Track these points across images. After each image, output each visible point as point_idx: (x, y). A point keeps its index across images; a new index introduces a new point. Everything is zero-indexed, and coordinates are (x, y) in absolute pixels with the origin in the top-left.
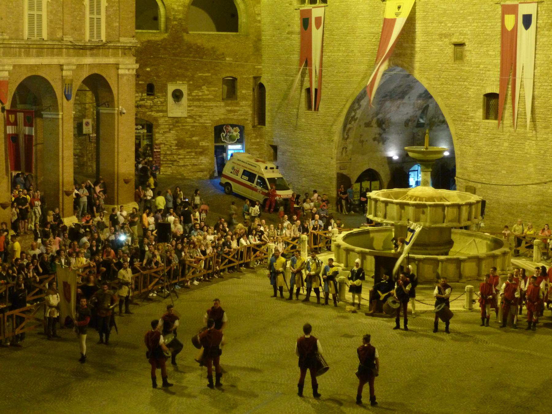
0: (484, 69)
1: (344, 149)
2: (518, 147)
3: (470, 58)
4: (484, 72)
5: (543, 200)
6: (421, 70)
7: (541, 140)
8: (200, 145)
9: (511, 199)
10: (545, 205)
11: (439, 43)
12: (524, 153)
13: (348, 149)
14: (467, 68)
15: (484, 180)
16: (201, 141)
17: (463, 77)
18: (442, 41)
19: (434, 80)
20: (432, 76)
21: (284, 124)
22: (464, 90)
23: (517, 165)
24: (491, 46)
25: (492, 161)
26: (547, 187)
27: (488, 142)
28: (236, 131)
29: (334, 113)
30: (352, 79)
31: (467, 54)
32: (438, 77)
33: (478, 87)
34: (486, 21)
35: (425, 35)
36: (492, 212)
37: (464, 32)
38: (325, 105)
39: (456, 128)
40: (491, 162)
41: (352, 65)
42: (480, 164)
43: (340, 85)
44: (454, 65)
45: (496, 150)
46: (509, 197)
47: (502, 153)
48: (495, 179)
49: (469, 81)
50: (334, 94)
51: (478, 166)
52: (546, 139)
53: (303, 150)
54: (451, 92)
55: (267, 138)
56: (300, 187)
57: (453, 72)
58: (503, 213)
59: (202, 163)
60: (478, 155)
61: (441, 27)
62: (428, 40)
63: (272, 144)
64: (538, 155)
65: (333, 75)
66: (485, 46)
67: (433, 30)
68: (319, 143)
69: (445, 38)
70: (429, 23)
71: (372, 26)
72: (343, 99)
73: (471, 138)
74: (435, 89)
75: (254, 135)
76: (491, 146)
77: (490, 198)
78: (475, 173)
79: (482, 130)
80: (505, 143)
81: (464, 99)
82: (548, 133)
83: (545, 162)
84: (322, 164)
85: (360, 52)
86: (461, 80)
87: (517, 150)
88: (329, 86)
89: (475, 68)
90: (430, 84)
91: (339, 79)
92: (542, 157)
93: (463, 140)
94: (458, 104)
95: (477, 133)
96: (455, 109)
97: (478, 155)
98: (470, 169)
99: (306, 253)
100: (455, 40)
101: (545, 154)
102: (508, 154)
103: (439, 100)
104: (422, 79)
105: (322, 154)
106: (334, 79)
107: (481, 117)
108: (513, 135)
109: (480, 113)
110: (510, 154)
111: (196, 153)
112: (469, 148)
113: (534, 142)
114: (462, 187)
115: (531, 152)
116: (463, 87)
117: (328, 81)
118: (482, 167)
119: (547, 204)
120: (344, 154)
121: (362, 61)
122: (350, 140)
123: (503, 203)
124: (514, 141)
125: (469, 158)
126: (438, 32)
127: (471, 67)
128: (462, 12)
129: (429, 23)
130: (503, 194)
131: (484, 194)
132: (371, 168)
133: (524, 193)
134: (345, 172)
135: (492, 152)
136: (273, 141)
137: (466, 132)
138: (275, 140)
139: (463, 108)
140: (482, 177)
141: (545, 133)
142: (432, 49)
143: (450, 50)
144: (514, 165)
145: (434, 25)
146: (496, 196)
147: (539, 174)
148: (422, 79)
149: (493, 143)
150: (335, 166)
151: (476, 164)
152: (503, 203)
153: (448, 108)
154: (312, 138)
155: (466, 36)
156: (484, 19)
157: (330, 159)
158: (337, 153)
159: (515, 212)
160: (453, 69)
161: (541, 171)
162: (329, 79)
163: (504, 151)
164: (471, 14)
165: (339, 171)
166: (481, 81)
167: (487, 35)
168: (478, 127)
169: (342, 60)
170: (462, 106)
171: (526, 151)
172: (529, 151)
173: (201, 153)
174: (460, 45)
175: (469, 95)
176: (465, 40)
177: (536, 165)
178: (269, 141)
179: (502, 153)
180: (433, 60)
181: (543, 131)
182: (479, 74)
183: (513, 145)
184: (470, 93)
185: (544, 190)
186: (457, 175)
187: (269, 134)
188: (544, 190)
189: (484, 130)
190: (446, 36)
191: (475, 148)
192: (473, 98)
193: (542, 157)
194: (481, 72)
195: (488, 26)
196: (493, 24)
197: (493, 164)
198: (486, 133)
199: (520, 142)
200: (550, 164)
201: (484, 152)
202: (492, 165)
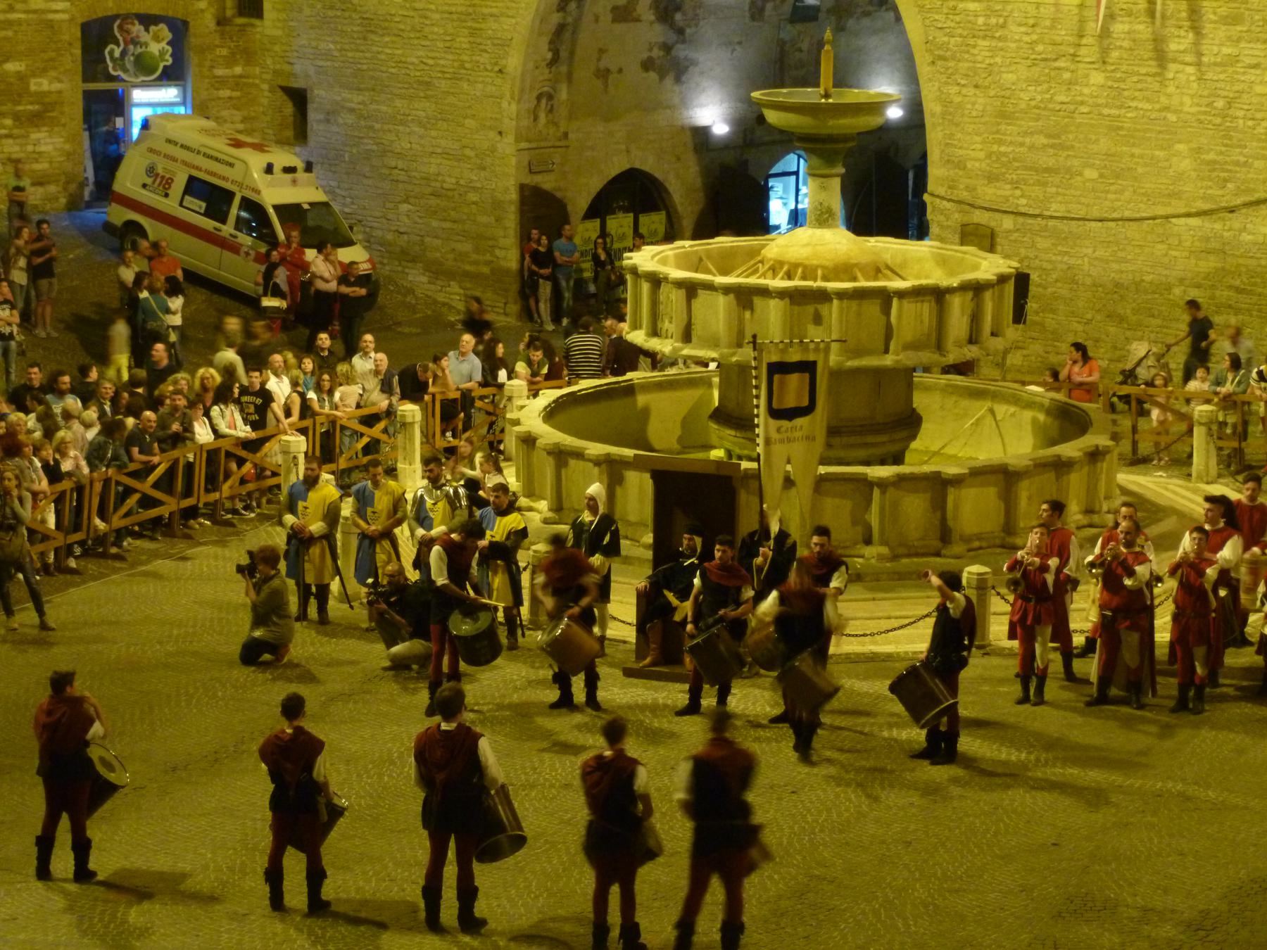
1: (544, 101)
2: (1139, 86)
5: (1223, 269)
7: (1215, 64)
8: (33, 88)
9: (1115, 266)
10: (1230, 287)
12: (1157, 106)
15: (1023, 201)
16: (34, 76)
21: (330, 13)
23: (1136, 151)
25: (1049, 136)
26: (1237, 225)
27: (1036, 70)
28: (157, 39)
36: (1054, 311)
39: (927, 22)
40: (1045, 141)
42: (1010, 149)
45: (1062, 98)
46: (1107, 262)
47: (1085, 109)
48: (1060, 198)
51: (1005, 154)
52: (1234, 60)
53: (398, 103)
55: (269, 61)
56: (390, 237)
58: (1089, 316)
59: (40, 153)
60: (1003, 115)
63: (284, 84)
64: (1205, 113)
68: (456, 78)
73: (979, 58)
75: (225, 52)
76: (1045, 86)
77: (1045, 265)
78: (992, 178)
79: (1014, 28)
80: (1094, 73)
82: (1239, 40)
83: (1231, 138)
84: (472, 154)
87: (1133, 99)
92: (1218, 120)
93: (951, 64)
95: (1000, 39)
97: (1003, 115)
98: (977, 165)
99: (418, 466)
101: (1231, 112)
102: (1106, 111)
108: (1121, 47)
110: (1113, 112)
111: (17, 117)
112: (972, 91)
113: (1190, 70)
114: (948, 227)
115: (1182, 104)
118: (1014, 159)
119: (1237, 283)
123: (1088, 281)
124: (1124, 68)
125: (970, 128)
130: (1090, 251)
131: (1023, 251)
132: (637, 165)
133: (1160, 246)
134: (547, 182)
135: (1051, 106)
136: (293, 75)
137: (961, 36)
138: (297, 68)
140: (1018, 192)
141: (1229, 38)
144: (1124, 148)
146: (1066, 259)
147: (1211, 180)
149: (1053, 74)
150: (513, 161)
151: (995, 148)
152: (1088, 281)
154: (431, 62)
158: (517, 115)
159: (1128, 311)
161: (1214, 170)
163: (1091, 101)
168: (1001, 20)
171: (1163, 99)
172: (1175, 101)
173: (36, 119)
177: (1199, 150)
178: (276, 72)
179: (1085, 109)
181: (1222, 32)
183: (1118, 80)
185: (1225, 234)
186: (930, 187)
187: (277, 48)
188: (1225, 234)
189: (1023, 29)
191: (992, 93)
193: (1218, 120)
197: (1052, 146)
198: (1027, 39)
199: (1143, 71)
200: (1245, 147)
201: (1023, 106)
202: (1051, 151)
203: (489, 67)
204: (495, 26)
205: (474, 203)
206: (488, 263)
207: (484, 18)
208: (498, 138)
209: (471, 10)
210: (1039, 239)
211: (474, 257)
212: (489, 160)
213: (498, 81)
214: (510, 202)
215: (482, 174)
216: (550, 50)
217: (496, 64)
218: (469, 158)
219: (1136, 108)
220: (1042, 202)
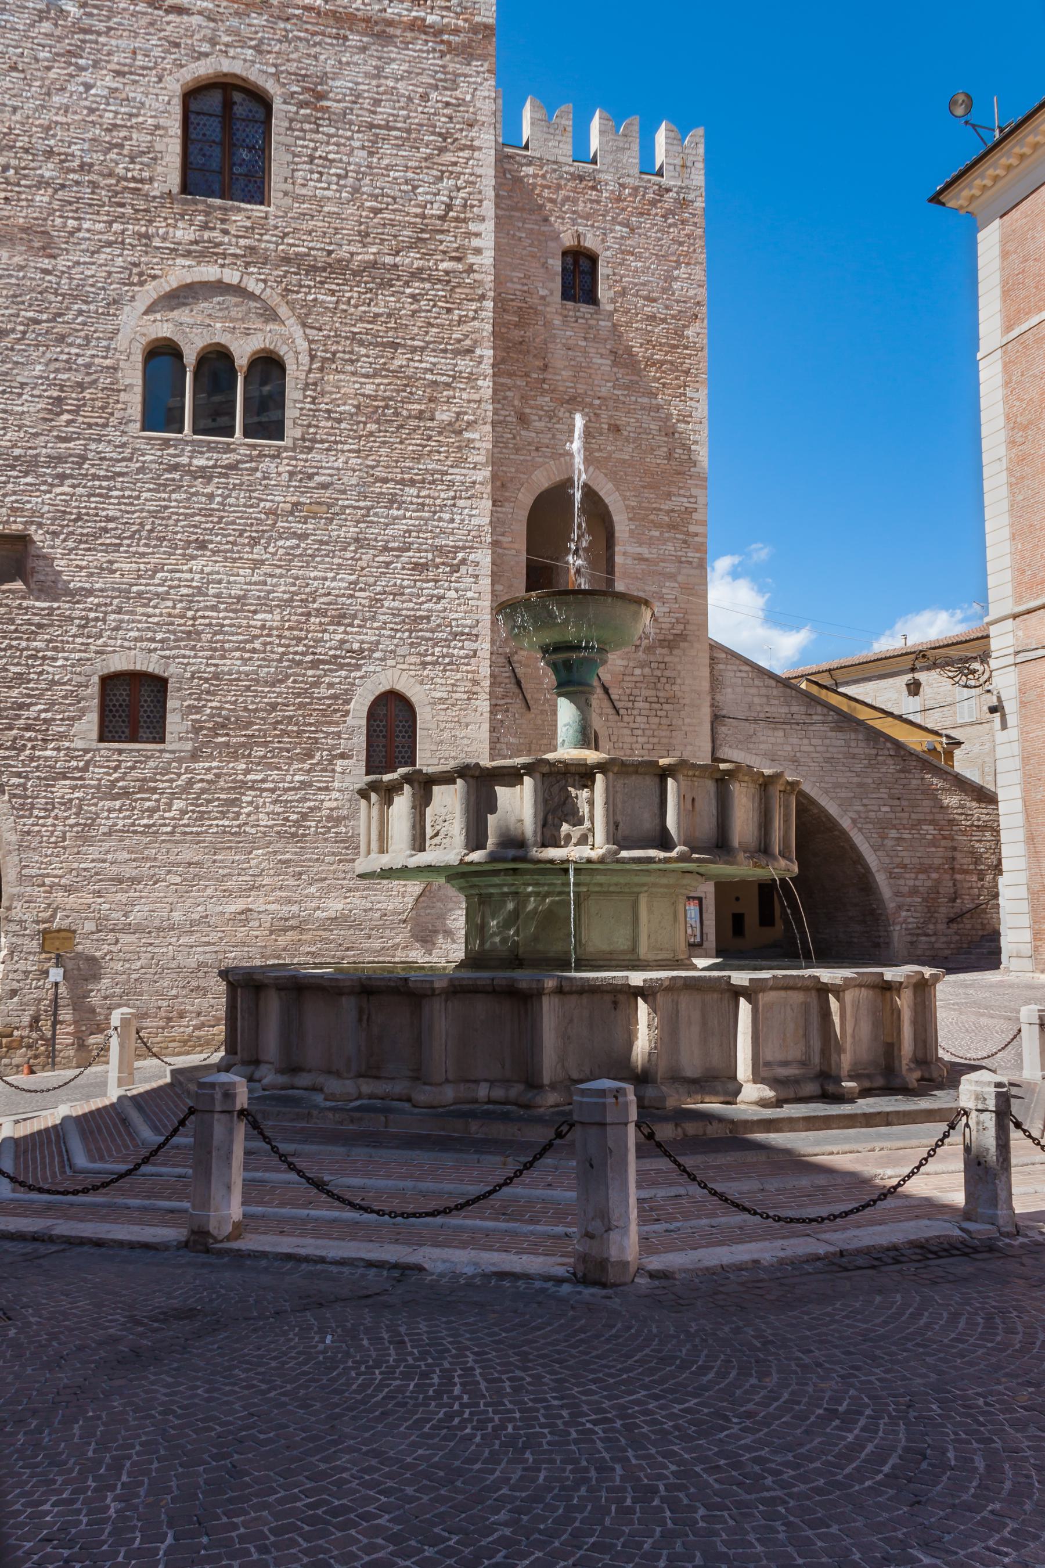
45: (145, 821)
92: (293, 830)
102: (188, 830)
107: (95, 735)
109: (90, 722)
110: (194, 829)
130: (174, 940)
156: (96, 478)
167: (109, 519)
168: (81, 764)
194: (92, 615)
195: (111, 497)
219: (217, 826)
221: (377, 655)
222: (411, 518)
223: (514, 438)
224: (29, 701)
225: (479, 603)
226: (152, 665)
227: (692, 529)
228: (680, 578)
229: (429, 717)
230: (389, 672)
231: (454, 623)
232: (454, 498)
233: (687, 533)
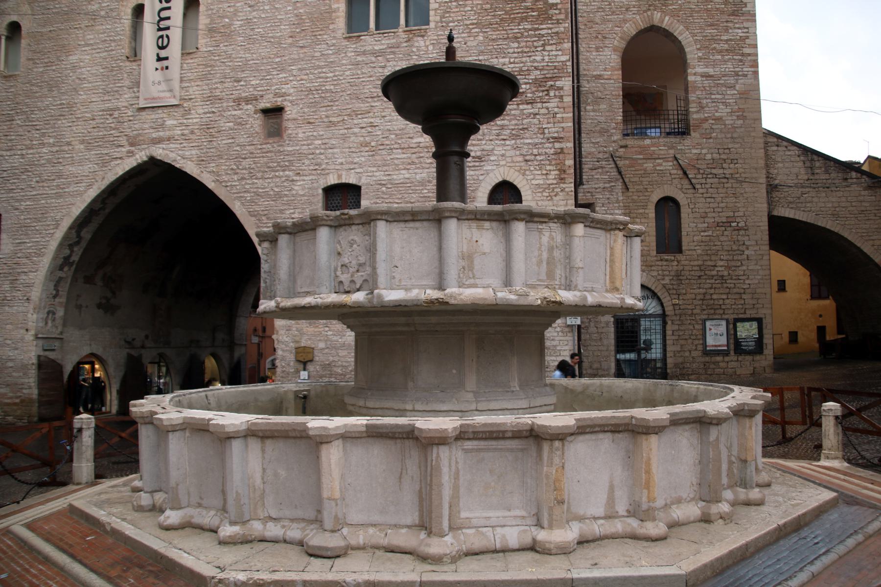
0: (323, 147)
1: (50, 315)
3: (296, 132)
4: (322, 151)
6: (203, 160)
11: (236, 112)
13: (57, 316)
14: (290, 149)
15: (331, 333)
17: (282, 163)
18: (240, 109)
19: (227, 174)
20: (223, 167)
22: (285, 184)
24: (334, 108)
29: (31, 251)
30: (66, 190)
31: (290, 125)
32: (235, 167)
33: (311, 177)
34: (324, 70)
35: (208, 103)
37: (283, 91)
38: (14, 239)
41: (67, 167)
43: (43, 202)
44: (264, 146)
49: (294, 168)
50: (30, 219)
54: (260, 190)
57: (263, 157)
61: (239, 88)
62: (213, 110)
65: (30, 186)
66: (324, 109)
67: (224, 94)
69: (247, 104)
70: (216, 83)
71: (106, 98)
72: (48, 225)
74: (228, 189)
77: (344, 364)
81: (285, 199)
84: (9, 342)
85: (82, 142)
86: (279, 168)
88: (21, 205)
89: (305, 147)
90: (218, 180)
91: (40, 192)
94: (275, 208)
96: (268, 218)
100: (265, 104)
103: (237, 207)
104: (202, 175)
105: (7, 324)
106: (32, 193)
114: (287, 350)
116: (284, 179)
117: (19, 198)
120: (50, 322)
121: (86, 157)
122: (61, 300)
126: (233, 96)
127: (297, 145)
128: (277, 60)
129: (216, 83)
134: (52, 355)
139: (283, 216)
140: (327, 329)
142: (222, 125)
143: (257, 123)
145: (226, 85)
148: (202, 175)
153: (253, 219)
155: (287, 98)
156: (320, 67)
157: (23, 331)
160: (264, 153)
162: (22, 194)
164: (294, 62)
165: (42, 353)
166: (317, 167)
169: (49, 161)
170: (282, 211)
174: (274, 113)
175: (294, 192)
176: (285, 103)
180: (224, 142)
182: (313, 156)
184: (296, 188)
190: (248, 101)
192: (303, 195)
194: (318, 152)
196: (337, 73)
203: (21, 298)
204: (24, 277)
205: (11, 367)
206: (17, 397)
207: (19, 273)
208: (25, 333)
209: (11, 271)
210: (340, 351)
211: (11, 395)
212: (19, 344)
213: (26, 304)
214: (33, 364)
215: (16, 352)
216: (55, 289)
217: (25, 296)
218: (8, 345)
220: (341, 332)
221: (492, 158)
222: (514, 63)
223: (610, 4)
224: (285, 207)
225: (564, 115)
226: (352, 180)
227: (747, 51)
228: (737, 87)
229: (530, 198)
230: (501, 169)
231: (546, 131)
232: (543, 45)
233: (743, 55)
